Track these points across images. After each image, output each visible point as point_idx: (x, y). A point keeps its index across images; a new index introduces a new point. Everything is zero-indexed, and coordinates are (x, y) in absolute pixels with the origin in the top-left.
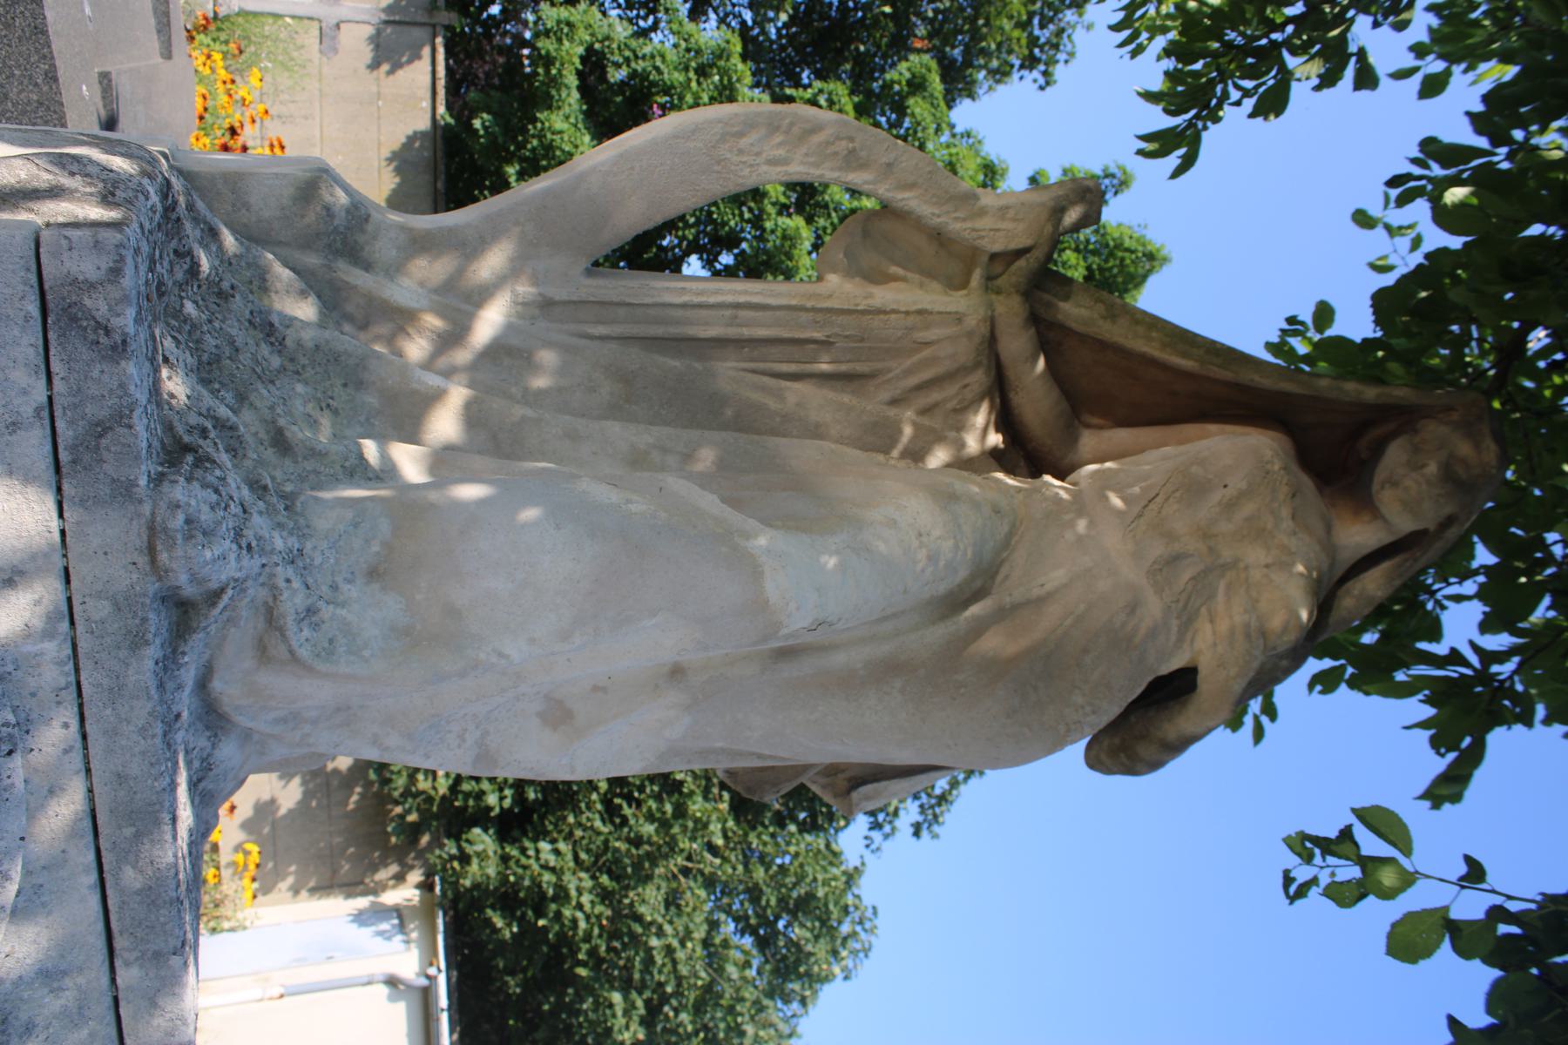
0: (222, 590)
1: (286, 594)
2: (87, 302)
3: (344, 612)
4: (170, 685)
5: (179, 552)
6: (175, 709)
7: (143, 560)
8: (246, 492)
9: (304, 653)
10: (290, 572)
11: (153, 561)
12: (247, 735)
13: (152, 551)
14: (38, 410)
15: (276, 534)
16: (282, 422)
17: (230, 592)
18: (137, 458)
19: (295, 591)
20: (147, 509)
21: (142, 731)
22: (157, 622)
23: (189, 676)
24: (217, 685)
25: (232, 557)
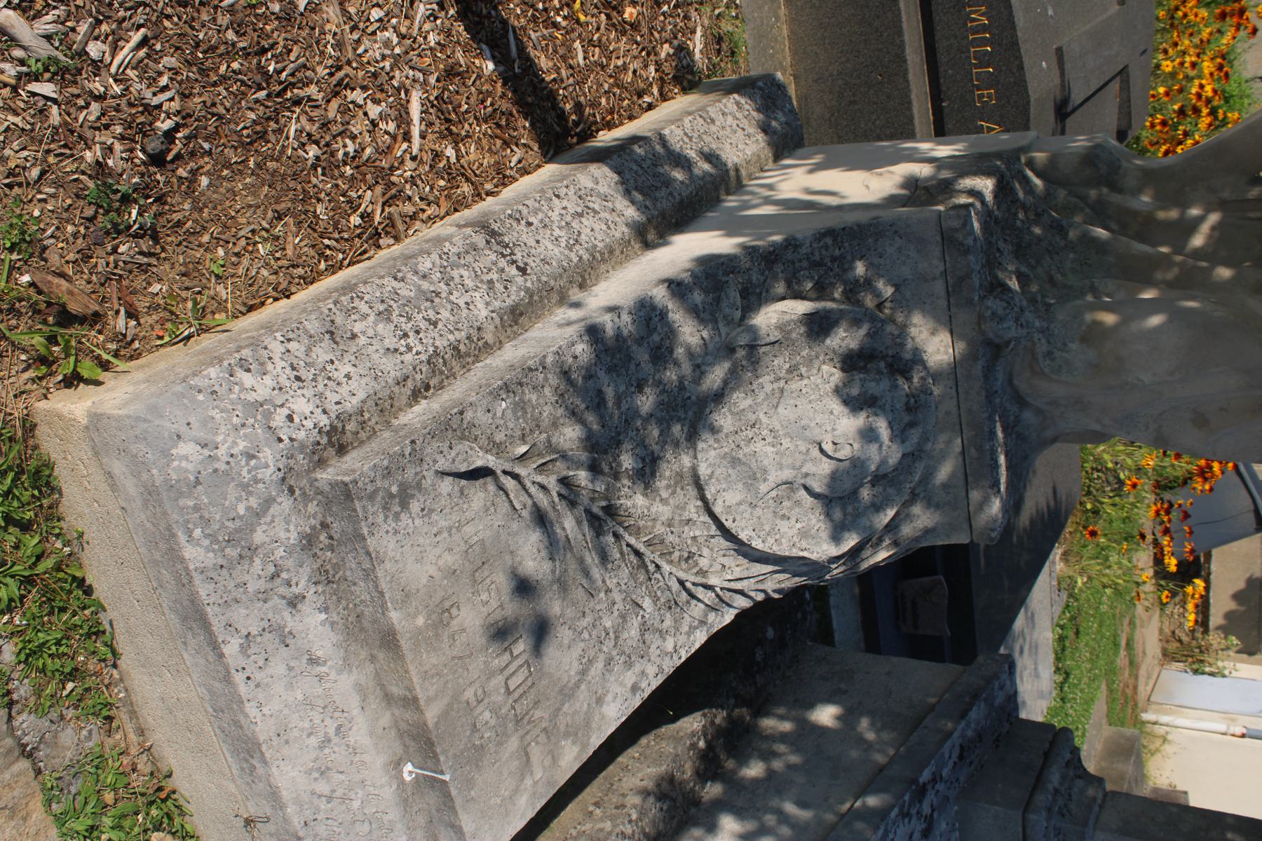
8: (1024, 303)
9: (1046, 370)
12: (1039, 412)
13: (979, 325)
23: (1001, 376)
24: (1016, 382)
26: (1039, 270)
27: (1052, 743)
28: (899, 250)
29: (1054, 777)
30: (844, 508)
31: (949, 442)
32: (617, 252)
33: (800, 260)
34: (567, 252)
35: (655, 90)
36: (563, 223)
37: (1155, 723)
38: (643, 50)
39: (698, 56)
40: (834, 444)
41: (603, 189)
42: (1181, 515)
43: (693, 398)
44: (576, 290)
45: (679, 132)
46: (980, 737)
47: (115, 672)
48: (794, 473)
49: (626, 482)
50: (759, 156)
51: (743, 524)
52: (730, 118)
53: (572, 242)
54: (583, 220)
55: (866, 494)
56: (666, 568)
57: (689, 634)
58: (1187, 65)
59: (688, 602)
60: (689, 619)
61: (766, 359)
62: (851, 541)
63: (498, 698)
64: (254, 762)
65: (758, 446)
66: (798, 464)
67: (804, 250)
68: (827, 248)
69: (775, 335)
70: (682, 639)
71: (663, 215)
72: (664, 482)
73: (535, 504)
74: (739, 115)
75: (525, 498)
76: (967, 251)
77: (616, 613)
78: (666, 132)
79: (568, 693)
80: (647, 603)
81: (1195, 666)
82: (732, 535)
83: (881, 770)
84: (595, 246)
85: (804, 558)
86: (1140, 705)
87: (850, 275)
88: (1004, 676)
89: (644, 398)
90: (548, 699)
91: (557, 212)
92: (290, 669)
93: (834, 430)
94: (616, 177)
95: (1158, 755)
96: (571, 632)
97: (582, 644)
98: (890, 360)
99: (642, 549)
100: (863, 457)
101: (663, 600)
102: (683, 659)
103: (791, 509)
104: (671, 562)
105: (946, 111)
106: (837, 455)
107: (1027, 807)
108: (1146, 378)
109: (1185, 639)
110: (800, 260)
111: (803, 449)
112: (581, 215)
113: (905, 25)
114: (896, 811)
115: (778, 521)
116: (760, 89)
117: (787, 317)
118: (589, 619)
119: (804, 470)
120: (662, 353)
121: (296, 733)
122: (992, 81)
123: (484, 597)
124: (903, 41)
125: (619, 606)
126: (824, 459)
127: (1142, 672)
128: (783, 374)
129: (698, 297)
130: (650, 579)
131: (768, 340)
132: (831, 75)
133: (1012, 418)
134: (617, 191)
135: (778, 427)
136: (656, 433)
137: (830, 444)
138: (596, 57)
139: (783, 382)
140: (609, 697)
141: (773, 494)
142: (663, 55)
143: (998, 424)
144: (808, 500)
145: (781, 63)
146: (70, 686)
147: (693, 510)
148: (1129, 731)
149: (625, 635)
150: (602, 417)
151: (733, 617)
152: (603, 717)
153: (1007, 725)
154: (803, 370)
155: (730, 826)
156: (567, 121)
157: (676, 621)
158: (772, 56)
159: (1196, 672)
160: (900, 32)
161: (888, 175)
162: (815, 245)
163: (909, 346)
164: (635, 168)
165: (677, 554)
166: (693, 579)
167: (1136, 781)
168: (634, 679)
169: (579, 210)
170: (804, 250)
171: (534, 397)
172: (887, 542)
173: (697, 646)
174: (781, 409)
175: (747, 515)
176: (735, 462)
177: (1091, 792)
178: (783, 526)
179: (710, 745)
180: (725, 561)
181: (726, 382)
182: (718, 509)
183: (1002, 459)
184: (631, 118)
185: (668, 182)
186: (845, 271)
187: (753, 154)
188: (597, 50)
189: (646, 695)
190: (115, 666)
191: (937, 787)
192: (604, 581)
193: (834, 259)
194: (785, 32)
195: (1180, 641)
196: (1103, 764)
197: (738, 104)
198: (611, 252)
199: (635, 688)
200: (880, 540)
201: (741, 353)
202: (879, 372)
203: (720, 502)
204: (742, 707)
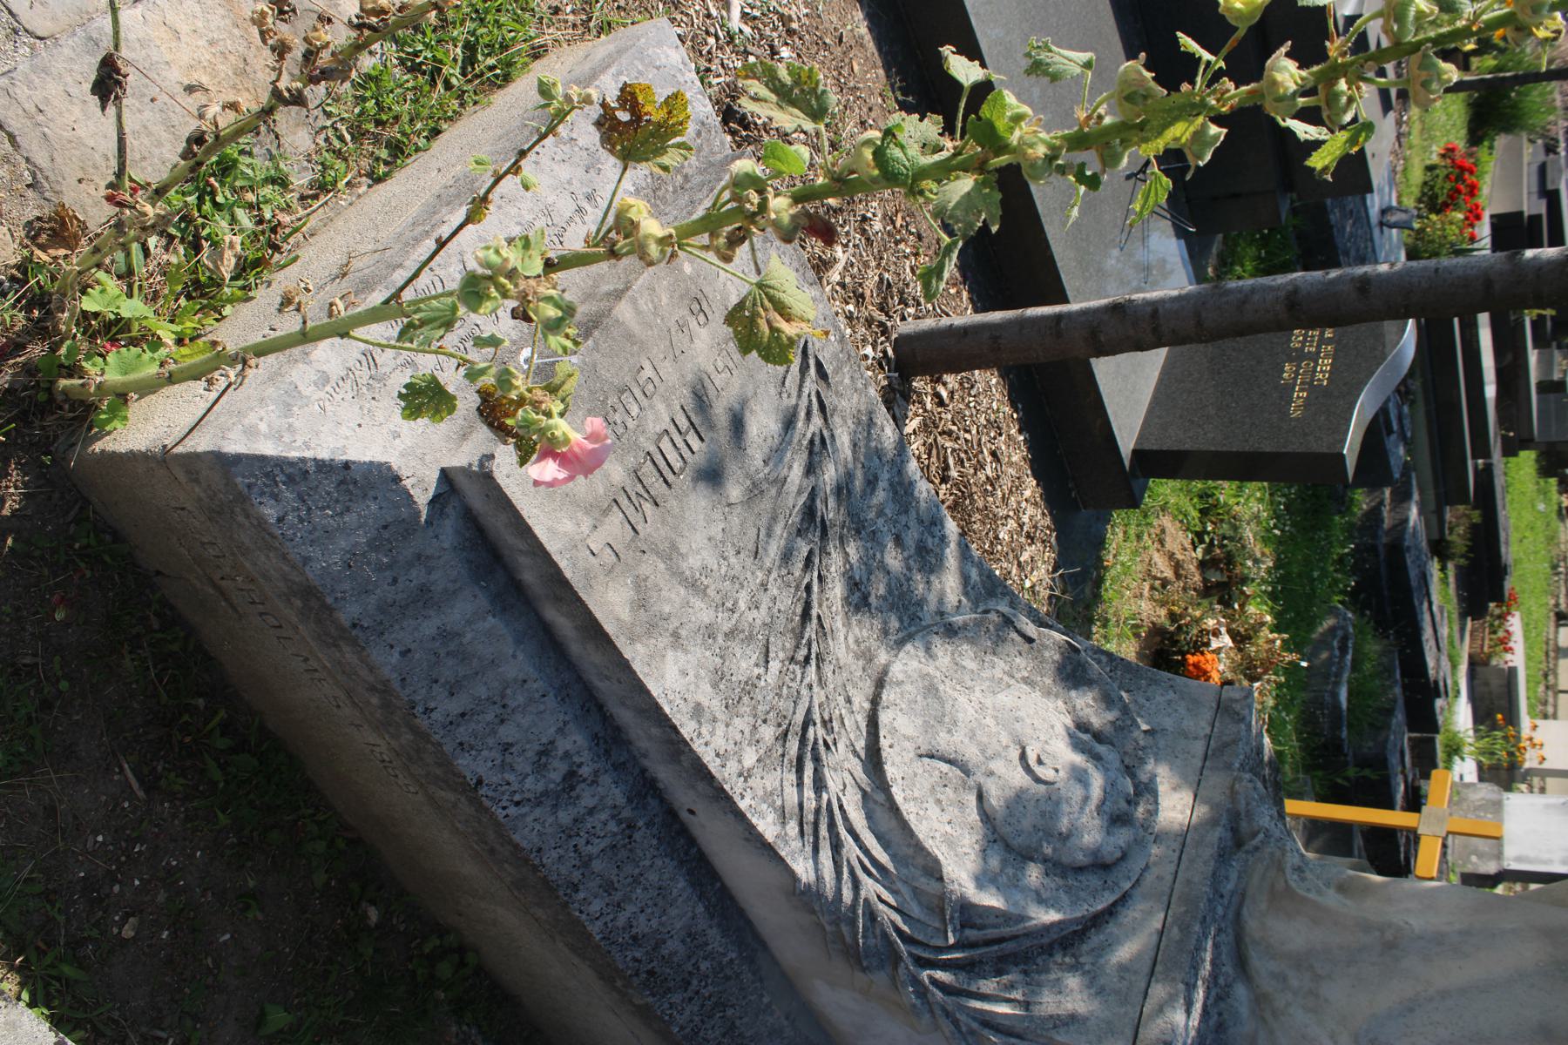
9: (1293, 885)
13: (1232, 787)
17: (1261, 836)
21: (1205, 863)
24: (1245, 911)
28: (1169, 702)
30: (1004, 862)
31: (1149, 913)
40: (1040, 762)
47: (364, 188)
51: (898, 760)
55: (1033, 874)
60: (777, 783)
61: (1009, 648)
62: (990, 900)
63: (654, 427)
64: (444, 211)
66: (990, 752)
72: (857, 630)
73: (796, 407)
75: (794, 394)
80: (775, 666)
85: (933, 870)
92: (569, 182)
99: (814, 612)
100: (1063, 792)
102: (743, 805)
108: (1417, 923)
119: (993, 765)
120: (927, 558)
121: (514, 211)
123: (720, 365)
126: (1020, 769)
129: (974, 574)
136: (882, 590)
139: (1012, 682)
141: (945, 767)
143: (1210, 943)
144: (973, 815)
146: (348, 137)
150: (864, 495)
171: (847, 381)
172: (1017, 995)
176: (931, 690)
178: (934, 811)
181: (965, 626)
182: (884, 718)
189: (698, 746)
190: (370, 186)
192: (770, 572)
199: (698, 711)
200: (1011, 986)
201: (993, 616)
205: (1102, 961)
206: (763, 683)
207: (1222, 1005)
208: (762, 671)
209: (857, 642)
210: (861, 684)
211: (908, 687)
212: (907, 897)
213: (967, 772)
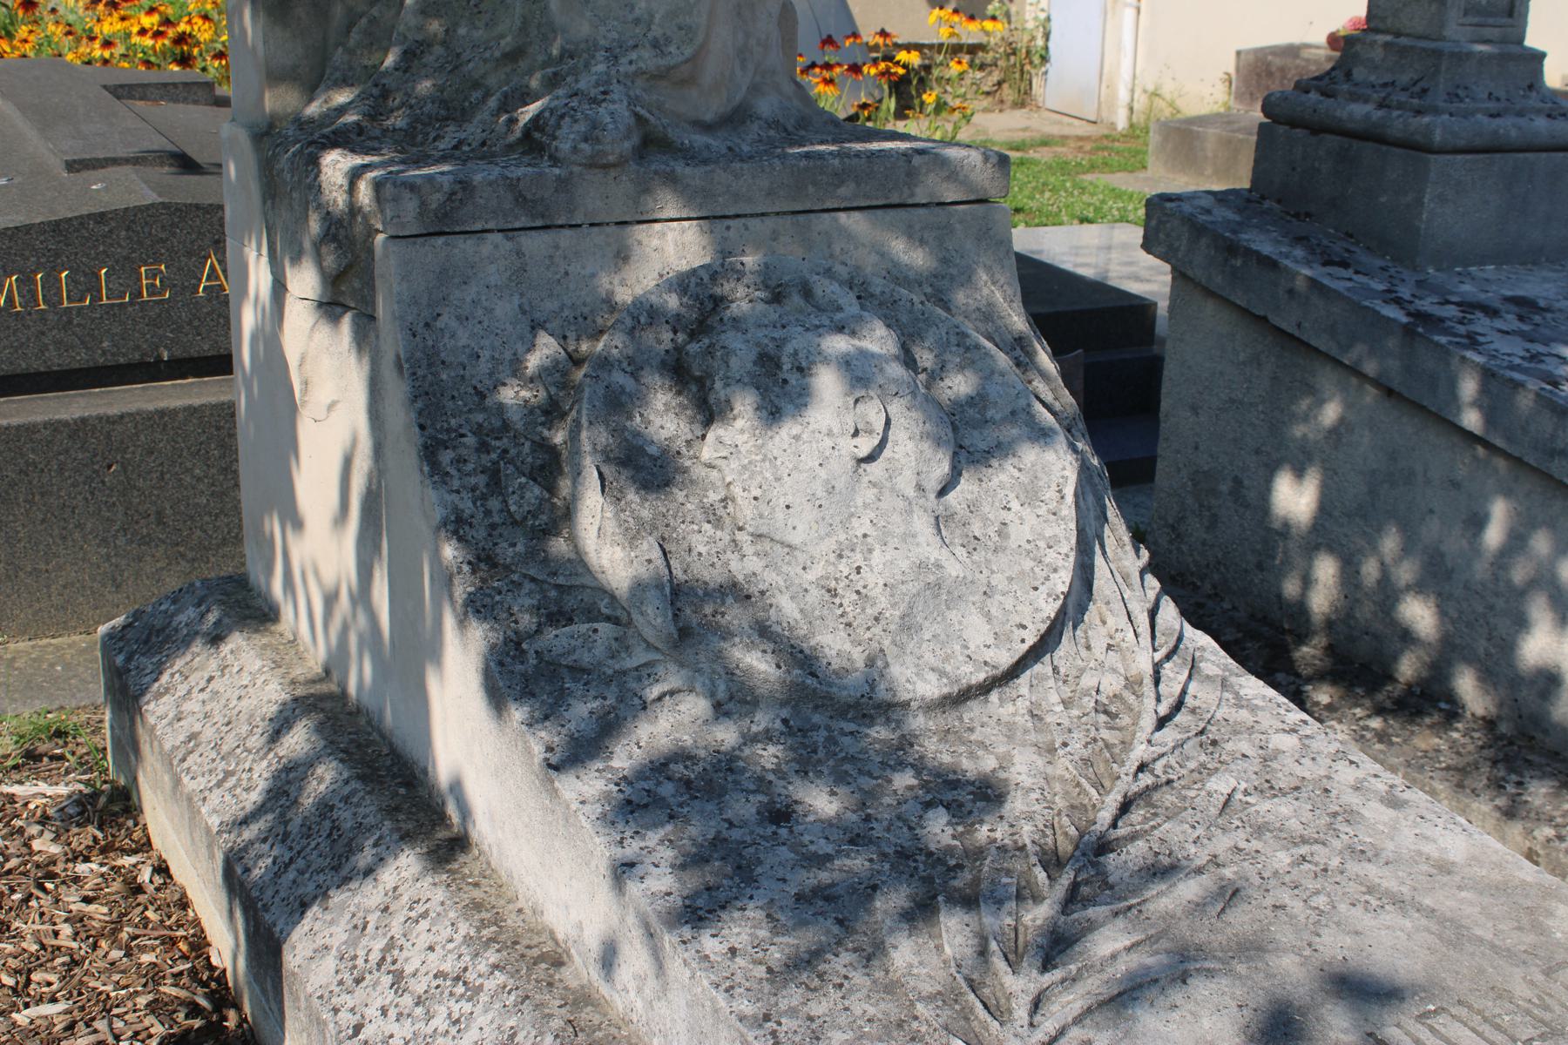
0: (636, 115)
1: (641, 65)
2: (434, 206)
3: (658, 16)
4: (705, 154)
5: (608, 148)
6: (724, 151)
7: (613, 173)
8: (560, 92)
9: (688, 51)
10: (624, 60)
11: (614, 165)
12: (755, 89)
14: (509, 239)
15: (594, 69)
16: (497, 54)
18: (541, 174)
19: (640, 57)
20: (576, 169)
22: (658, 163)
23: (700, 139)
24: (708, 117)
25: (611, 107)
26: (492, 81)
27: (1293, 123)
28: (463, 319)
29: (1358, 112)
32: (477, 894)
33: (488, 513)
34: (484, 998)
35: (128, 861)
36: (419, 1011)
37: (1131, 109)
38: (44, 890)
39: (62, 790)
40: (856, 433)
41: (338, 935)
42: (828, 49)
43: (785, 713)
44: (566, 973)
45: (215, 798)
46: (1299, 240)
48: (918, 512)
49: (982, 833)
50: (264, 647)
51: (1026, 609)
52: (187, 707)
53: (460, 989)
54: (409, 969)
56: (1140, 752)
57: (1253, 709)
58: (107, 54)
59: (1193, 711)
65: (873, 579)
66: (901, 504)
67: (467, 506)
68: (461, 461)
69: (649, 548)
70: (1266, 721)
71: (392, 811)
72: (966, 764)
74: (182, 690)
76: (465, 185)
77: (1256, 844)
78: (214, 822)
79: (1453, 933)
80: (1221, 785)
81: (1037, 60)
82: (1049, 630)
83: (1389, 392)
84: (468, 939)
85: (1076, 495)
86: (1106, 132)
87: (515, 417)
88: (1187, 208)
89: (799, 808)
90: (1482, 971)
91: (393, 1027)
93: (830, 434)
94: (315, 909)
95: (1179, 103)
96: (1325, 931)
97: (1343, 907)
98: (681, 337)
99: (1113, 800)
101: (1203, 758)
103: (985, 519)
104: (1127, 745)
105: (178, 353)
106: (879, 425)
107: (1419, 147)
109: (996, 76)
110: (488, 513)
111: (870, 494)
112: (398, 977)
113: (15, 421)
114: (1469, 354)
115: (1013, 543)
116: (129, 659)
117: (611, 526)
118: (1285, 897)
119: (911, 492)
122: (126, 269)
124: (46, 425)
125: (1239, 838)
126: (887, 453)
127: (1055, 130)
128: (724, 536)
130: (1169, 782)
131: (659, 561)
132: (108, 557)
133: (772, 133)
134: (343, 907)
135: (829, 545)
137: (857, 441)
138: (53, 978)
139: (740, 536)
140: (1428, 848)
142: (55, 849)
144: (967, 487)
145: (82, 651)
147: (1010, 708)
148: (1154, 138)
149: (1293, 824)
151: (1199, 633)
152: (1473, 860)
153: (1267, 204)
154: (713, 497)
155: (1542, 644)
156: (189, 1030)
157: (1236, 733)
158: (67, 666)
159: (1045, 59)
160: (31, 429)
161: (307, 367)
162: (456, 484)
163: (654, 299)
164: (291, 875)
165: (1105, 734)
166: (1149, 701)
167: (1229, 123)
168: (1375, 804)
169: (387, 980)
170: (467, 506)
173: (1271, 692)
174: (795, 538)
175: (1009, 602)
176: (908, 625)
177: (1378, 54)
178: (1019, 534)
179: (1379, 711)
180: (1099, 645)
182: (1005, 659)
183: (858, 146)
184: (184, 904)
185: (325, 807)
186: (506, 426)
187: (261, 656)
188: (35, 977)
191: (1407, 296)
193: (484, 447)
194: (23, 645)
195: (999, 84)
196: (1209, 171)
197: (159, 696)
198: (477, 906)
199: (1393, 802)
202: (709, 351)
203: (989, 655)
204: (1291, 662)
205: (911, 274)
206: (1243, 785)
207: (790, 128)
208: (1239, 796)
209: (972, 755)
210: (992, 722)
211: (929, 657)
212: (1092, 514)
213: (937, 518)
